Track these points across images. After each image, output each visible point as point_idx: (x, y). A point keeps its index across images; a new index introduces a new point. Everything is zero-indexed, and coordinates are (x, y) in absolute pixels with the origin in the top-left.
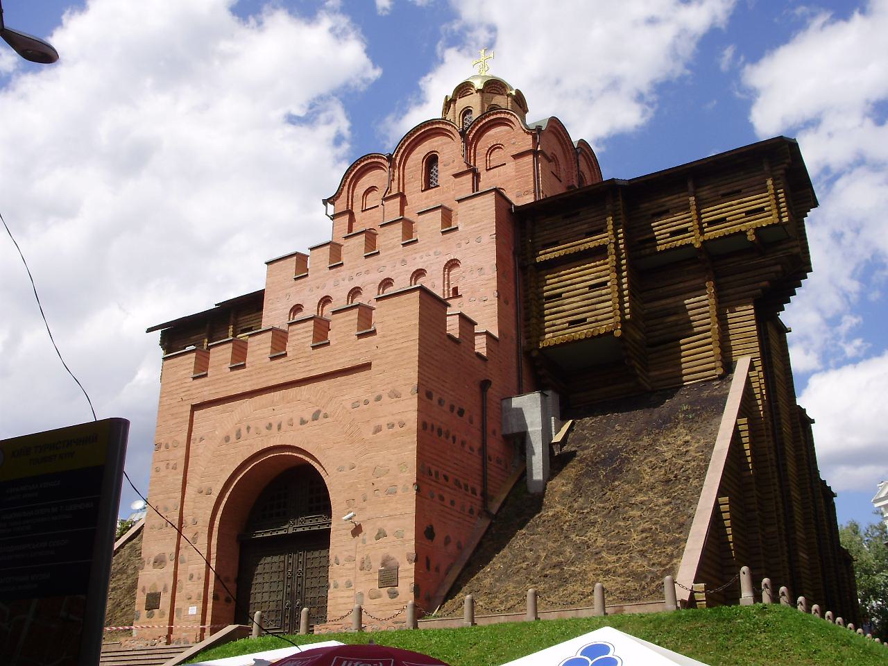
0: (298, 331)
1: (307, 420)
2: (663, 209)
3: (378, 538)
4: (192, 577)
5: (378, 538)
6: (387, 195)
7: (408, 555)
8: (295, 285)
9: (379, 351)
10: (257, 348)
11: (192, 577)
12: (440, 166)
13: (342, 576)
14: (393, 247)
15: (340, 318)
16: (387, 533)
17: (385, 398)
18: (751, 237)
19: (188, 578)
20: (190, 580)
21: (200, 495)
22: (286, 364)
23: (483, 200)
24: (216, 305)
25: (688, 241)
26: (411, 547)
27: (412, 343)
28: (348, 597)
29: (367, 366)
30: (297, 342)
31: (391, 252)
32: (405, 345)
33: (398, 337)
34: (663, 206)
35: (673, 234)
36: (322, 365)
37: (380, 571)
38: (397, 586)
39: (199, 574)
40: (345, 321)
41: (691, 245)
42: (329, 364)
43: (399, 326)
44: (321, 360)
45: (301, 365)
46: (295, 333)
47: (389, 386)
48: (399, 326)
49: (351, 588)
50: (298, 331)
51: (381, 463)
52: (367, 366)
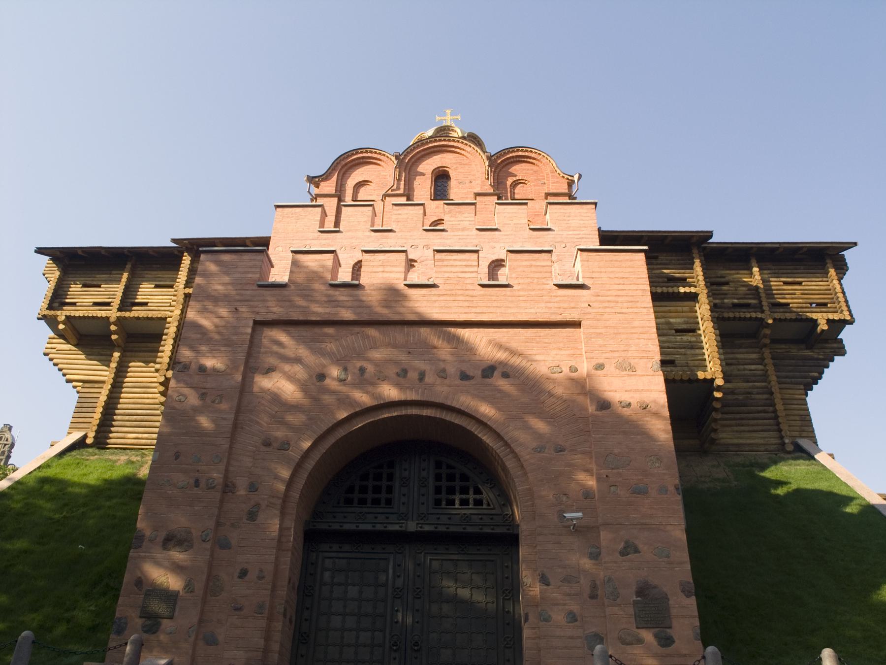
0: (452, 263)
1: (472, 374)
2: (723, 280)
3: (624, 553)
4: (243, 573)
5: (624, 553)
6: (390, 192)
7: (682, 584)
8: (318, 238)
9: (589, 310)
10: (381, 269)
11: (243, 573)
12: (453, 183)
13: (557, 604)
14: (463, 229)
15: (522, 261)
16: (641, 547)
17: (610, 368)
18: (823, 326)
19: (237, 575)
20: (240, 577)
21: (264, 448)
22: (434, 298)
23: (581, 210)
24: (174, 241)
25: (759, 315)
26: (684, 571)
27: (645, 310)
28: (571, 638)
29: (577, 324)
30: (451, 275)
31: (460, 233)
32: (630, 310)
33: (620, 299)
34: (724, 277)
35: (735, 306)
36: (498, 311)
37: (635, 603)
38: (670, 627)
39: (261, 571)
40: (531, 266)
41: (762, 320)
42: (510, 311)
43: (621, 287)
44: (495, 304)
45: (461, 304)
46: (445, 263)
47: (616, 355)
48: (621, 287)
49: (576, 623)
50: (452, 263)
51: (616, 451)
52: (577, 324)
